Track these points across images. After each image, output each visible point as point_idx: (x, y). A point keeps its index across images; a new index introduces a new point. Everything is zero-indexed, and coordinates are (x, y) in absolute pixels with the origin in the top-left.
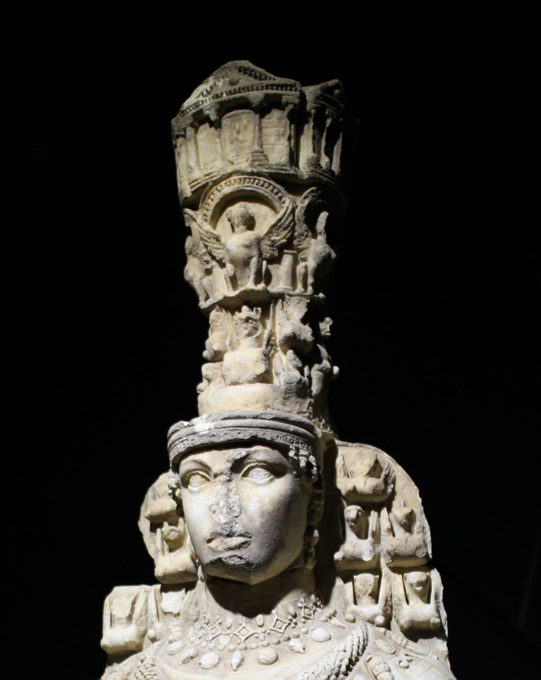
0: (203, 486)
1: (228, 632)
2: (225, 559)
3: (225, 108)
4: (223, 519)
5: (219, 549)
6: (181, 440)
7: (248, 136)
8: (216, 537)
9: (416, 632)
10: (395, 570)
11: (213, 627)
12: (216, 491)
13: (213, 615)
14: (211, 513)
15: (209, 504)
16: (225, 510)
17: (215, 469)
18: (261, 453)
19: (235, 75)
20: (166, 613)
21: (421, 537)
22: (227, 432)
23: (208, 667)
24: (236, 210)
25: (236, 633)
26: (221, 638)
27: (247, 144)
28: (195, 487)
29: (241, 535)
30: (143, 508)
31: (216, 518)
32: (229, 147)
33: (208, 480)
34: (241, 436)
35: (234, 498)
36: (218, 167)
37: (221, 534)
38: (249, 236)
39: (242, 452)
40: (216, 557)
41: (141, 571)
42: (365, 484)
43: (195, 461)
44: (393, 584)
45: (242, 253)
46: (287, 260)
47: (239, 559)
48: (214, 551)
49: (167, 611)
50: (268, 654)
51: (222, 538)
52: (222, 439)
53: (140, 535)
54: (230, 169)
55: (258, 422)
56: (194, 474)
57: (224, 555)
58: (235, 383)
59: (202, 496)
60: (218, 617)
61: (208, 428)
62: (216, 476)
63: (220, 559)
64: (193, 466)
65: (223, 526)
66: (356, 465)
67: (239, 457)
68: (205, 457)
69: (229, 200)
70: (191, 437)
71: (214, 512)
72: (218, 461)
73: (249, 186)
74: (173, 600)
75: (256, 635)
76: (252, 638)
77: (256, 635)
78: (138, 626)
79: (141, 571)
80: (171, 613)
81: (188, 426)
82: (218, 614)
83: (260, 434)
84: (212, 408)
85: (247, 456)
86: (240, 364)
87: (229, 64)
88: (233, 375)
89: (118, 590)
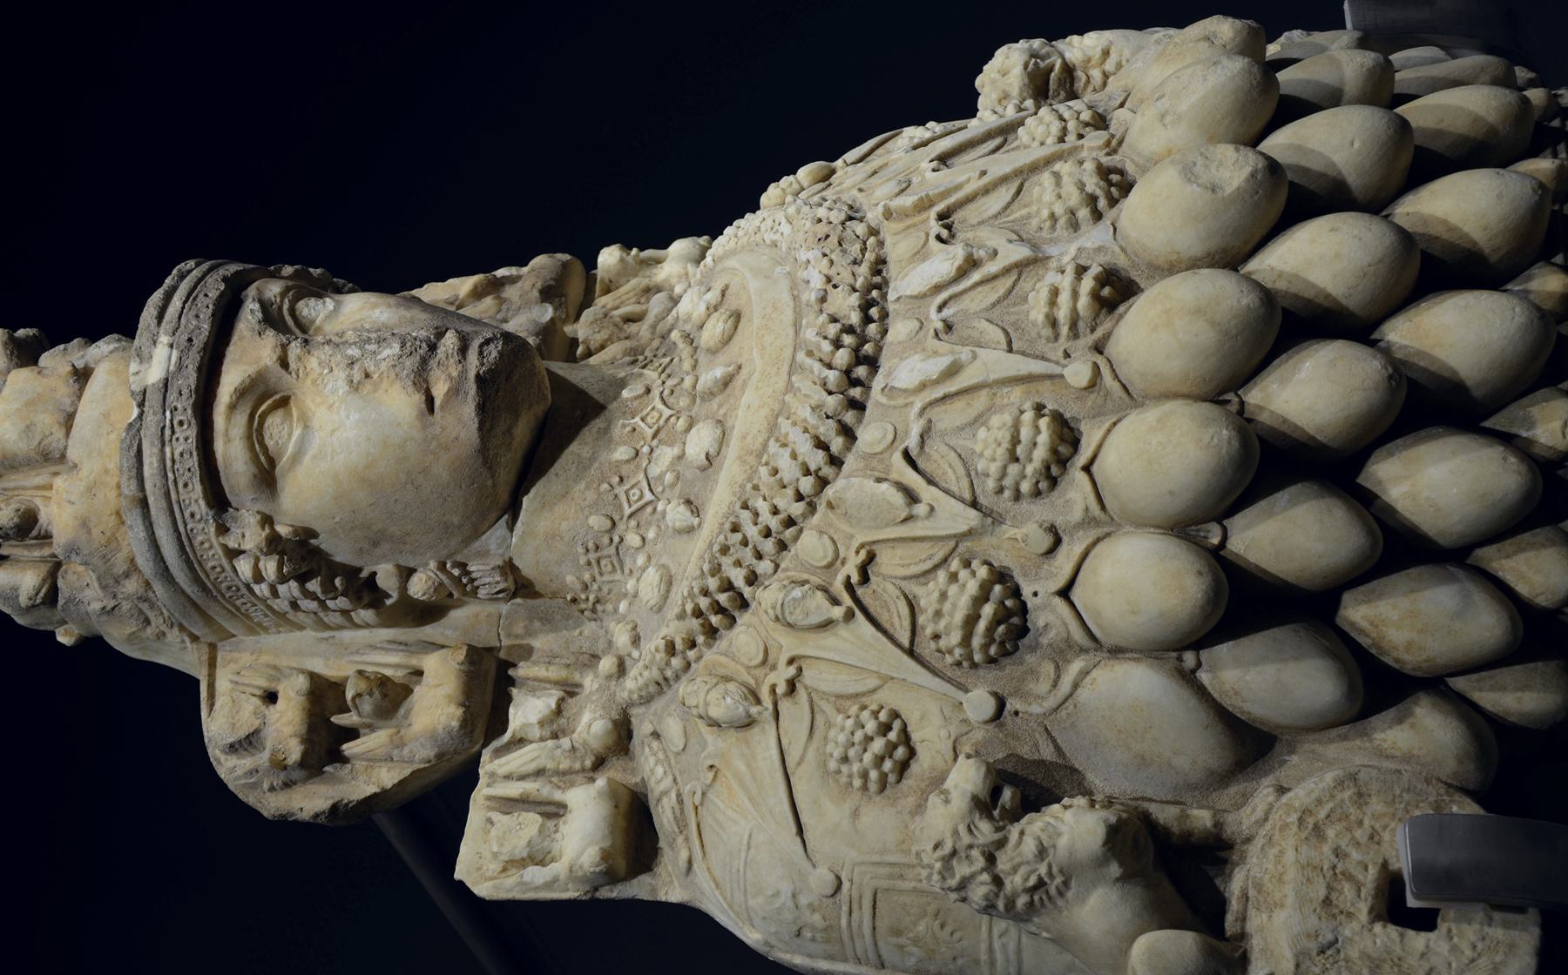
0: (295, 414)
1: (646, 449)
2: (482, 365)
5: (455, 374)
6: (168, 432)
8: (426, 381)
11: (623, 498)
12: (318, 370)
13: (594, 507)
14: (368, 387)
15: (343, 387)
16: (372, 347)
20: (559, 711)
22: (193, 312)
23: (719, 431)
25: (649, 432)
26: (654, 471)
28: (290, 435)
29: (440, 335)
31: (383, 366)
33: (284, 402)
34: (213, 294)
37: (424, 361)
40: (471, 387)
43: (232, 407)
47: (492, 346)
48: (455, 391)
49: (554, 706)
51: (433, 363)
52: (206, 327)
56: (261, 425)
58: (69, 420)
59: (322, 417)
60: (605, 486)
61: (167, 349)
62: (284, 364)
63: (478, 376)
64: (241, 419)
65: (407, 351)
67: (260, 315)
68: (231, 379)
70: (172, 397)
71: (367, 376)
72: (251, 353)
74: (526, 711)
75: (666, 392)
76: (671, 400)
77: (666, 392)
78: (572, 785)
80: (560, 702)
81: (141, 405)
82: (597, 489)
84: (106, 471)
85: (265, 306)
86: (30, 404)
88: (47, 421)
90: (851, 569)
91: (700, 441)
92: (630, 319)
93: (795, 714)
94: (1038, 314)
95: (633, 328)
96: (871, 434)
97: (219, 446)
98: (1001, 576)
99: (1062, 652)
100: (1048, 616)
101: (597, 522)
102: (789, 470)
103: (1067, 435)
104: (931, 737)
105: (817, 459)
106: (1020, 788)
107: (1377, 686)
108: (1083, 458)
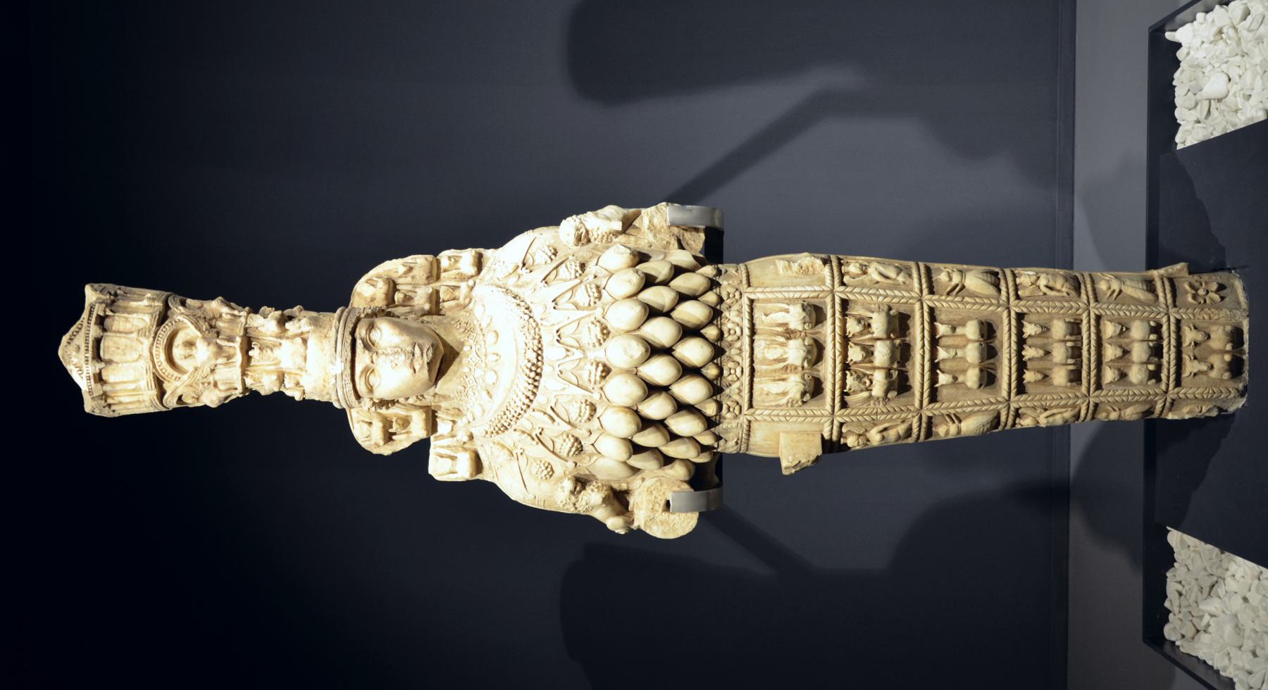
3: (97, 357)
4: (403, 357)
7: (122, 341)
9: (479, 264)
10: (438, 278)
17: (368, 361)
18: (361, 332)
19: (72, 348)
21: (420, 261)
24: (178, 352)
27: (129, 343)
30: (375, 451)
32: (128, 358)
35: (389, 351)
36: (144, 364)
38: (201, 345)
39: (359, 342)
41: (422, 447)
42: (381, 289)
44: (447, 279)
45: (212, 349)
46: (220, 324)
48: (422, 368)
50: (490, 337)
53: (395, 454)
54: (146, 353)
55: (341, 330)
57: (426, 360)
66: (368, 290)
69: (170, 360)
72: (363, 359)
73: (163, 340)
74: (443, 427)
79: (422, 447)
83: (349, 329)
87: (60, 353)
88: (299, 360)
89: (431, 471)
90: (537, 432)
91: (490, 378)
92: (456, 288)
93: (522, 460)
94: (585, 377)
95: (456, 293)
96: (540, 400)
97: (358, 387)
98: (577, 440)
99: (591, 456)
100: (588, 448)
101: (461, 388)
102: (520, 404)
103: (594, 409)
104: (559, 470)
105: (527, 401)
106: (581, 482)
107: (667, 461)
108: (598, 415)
